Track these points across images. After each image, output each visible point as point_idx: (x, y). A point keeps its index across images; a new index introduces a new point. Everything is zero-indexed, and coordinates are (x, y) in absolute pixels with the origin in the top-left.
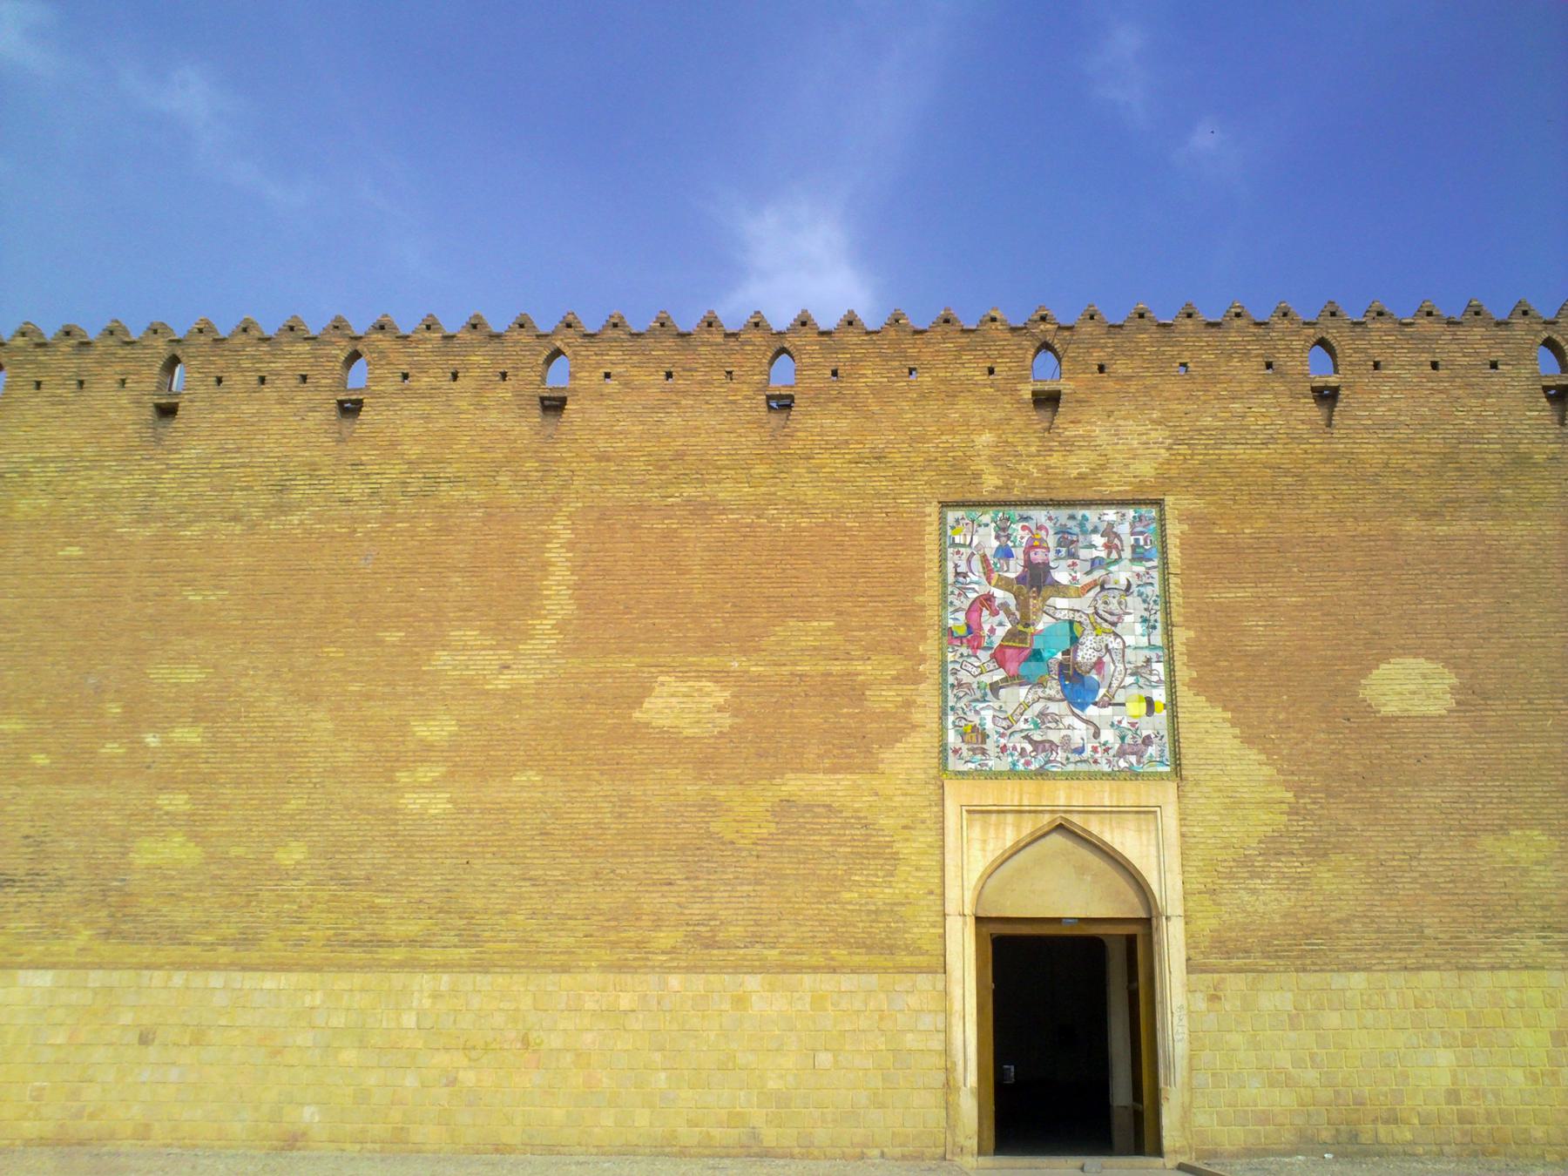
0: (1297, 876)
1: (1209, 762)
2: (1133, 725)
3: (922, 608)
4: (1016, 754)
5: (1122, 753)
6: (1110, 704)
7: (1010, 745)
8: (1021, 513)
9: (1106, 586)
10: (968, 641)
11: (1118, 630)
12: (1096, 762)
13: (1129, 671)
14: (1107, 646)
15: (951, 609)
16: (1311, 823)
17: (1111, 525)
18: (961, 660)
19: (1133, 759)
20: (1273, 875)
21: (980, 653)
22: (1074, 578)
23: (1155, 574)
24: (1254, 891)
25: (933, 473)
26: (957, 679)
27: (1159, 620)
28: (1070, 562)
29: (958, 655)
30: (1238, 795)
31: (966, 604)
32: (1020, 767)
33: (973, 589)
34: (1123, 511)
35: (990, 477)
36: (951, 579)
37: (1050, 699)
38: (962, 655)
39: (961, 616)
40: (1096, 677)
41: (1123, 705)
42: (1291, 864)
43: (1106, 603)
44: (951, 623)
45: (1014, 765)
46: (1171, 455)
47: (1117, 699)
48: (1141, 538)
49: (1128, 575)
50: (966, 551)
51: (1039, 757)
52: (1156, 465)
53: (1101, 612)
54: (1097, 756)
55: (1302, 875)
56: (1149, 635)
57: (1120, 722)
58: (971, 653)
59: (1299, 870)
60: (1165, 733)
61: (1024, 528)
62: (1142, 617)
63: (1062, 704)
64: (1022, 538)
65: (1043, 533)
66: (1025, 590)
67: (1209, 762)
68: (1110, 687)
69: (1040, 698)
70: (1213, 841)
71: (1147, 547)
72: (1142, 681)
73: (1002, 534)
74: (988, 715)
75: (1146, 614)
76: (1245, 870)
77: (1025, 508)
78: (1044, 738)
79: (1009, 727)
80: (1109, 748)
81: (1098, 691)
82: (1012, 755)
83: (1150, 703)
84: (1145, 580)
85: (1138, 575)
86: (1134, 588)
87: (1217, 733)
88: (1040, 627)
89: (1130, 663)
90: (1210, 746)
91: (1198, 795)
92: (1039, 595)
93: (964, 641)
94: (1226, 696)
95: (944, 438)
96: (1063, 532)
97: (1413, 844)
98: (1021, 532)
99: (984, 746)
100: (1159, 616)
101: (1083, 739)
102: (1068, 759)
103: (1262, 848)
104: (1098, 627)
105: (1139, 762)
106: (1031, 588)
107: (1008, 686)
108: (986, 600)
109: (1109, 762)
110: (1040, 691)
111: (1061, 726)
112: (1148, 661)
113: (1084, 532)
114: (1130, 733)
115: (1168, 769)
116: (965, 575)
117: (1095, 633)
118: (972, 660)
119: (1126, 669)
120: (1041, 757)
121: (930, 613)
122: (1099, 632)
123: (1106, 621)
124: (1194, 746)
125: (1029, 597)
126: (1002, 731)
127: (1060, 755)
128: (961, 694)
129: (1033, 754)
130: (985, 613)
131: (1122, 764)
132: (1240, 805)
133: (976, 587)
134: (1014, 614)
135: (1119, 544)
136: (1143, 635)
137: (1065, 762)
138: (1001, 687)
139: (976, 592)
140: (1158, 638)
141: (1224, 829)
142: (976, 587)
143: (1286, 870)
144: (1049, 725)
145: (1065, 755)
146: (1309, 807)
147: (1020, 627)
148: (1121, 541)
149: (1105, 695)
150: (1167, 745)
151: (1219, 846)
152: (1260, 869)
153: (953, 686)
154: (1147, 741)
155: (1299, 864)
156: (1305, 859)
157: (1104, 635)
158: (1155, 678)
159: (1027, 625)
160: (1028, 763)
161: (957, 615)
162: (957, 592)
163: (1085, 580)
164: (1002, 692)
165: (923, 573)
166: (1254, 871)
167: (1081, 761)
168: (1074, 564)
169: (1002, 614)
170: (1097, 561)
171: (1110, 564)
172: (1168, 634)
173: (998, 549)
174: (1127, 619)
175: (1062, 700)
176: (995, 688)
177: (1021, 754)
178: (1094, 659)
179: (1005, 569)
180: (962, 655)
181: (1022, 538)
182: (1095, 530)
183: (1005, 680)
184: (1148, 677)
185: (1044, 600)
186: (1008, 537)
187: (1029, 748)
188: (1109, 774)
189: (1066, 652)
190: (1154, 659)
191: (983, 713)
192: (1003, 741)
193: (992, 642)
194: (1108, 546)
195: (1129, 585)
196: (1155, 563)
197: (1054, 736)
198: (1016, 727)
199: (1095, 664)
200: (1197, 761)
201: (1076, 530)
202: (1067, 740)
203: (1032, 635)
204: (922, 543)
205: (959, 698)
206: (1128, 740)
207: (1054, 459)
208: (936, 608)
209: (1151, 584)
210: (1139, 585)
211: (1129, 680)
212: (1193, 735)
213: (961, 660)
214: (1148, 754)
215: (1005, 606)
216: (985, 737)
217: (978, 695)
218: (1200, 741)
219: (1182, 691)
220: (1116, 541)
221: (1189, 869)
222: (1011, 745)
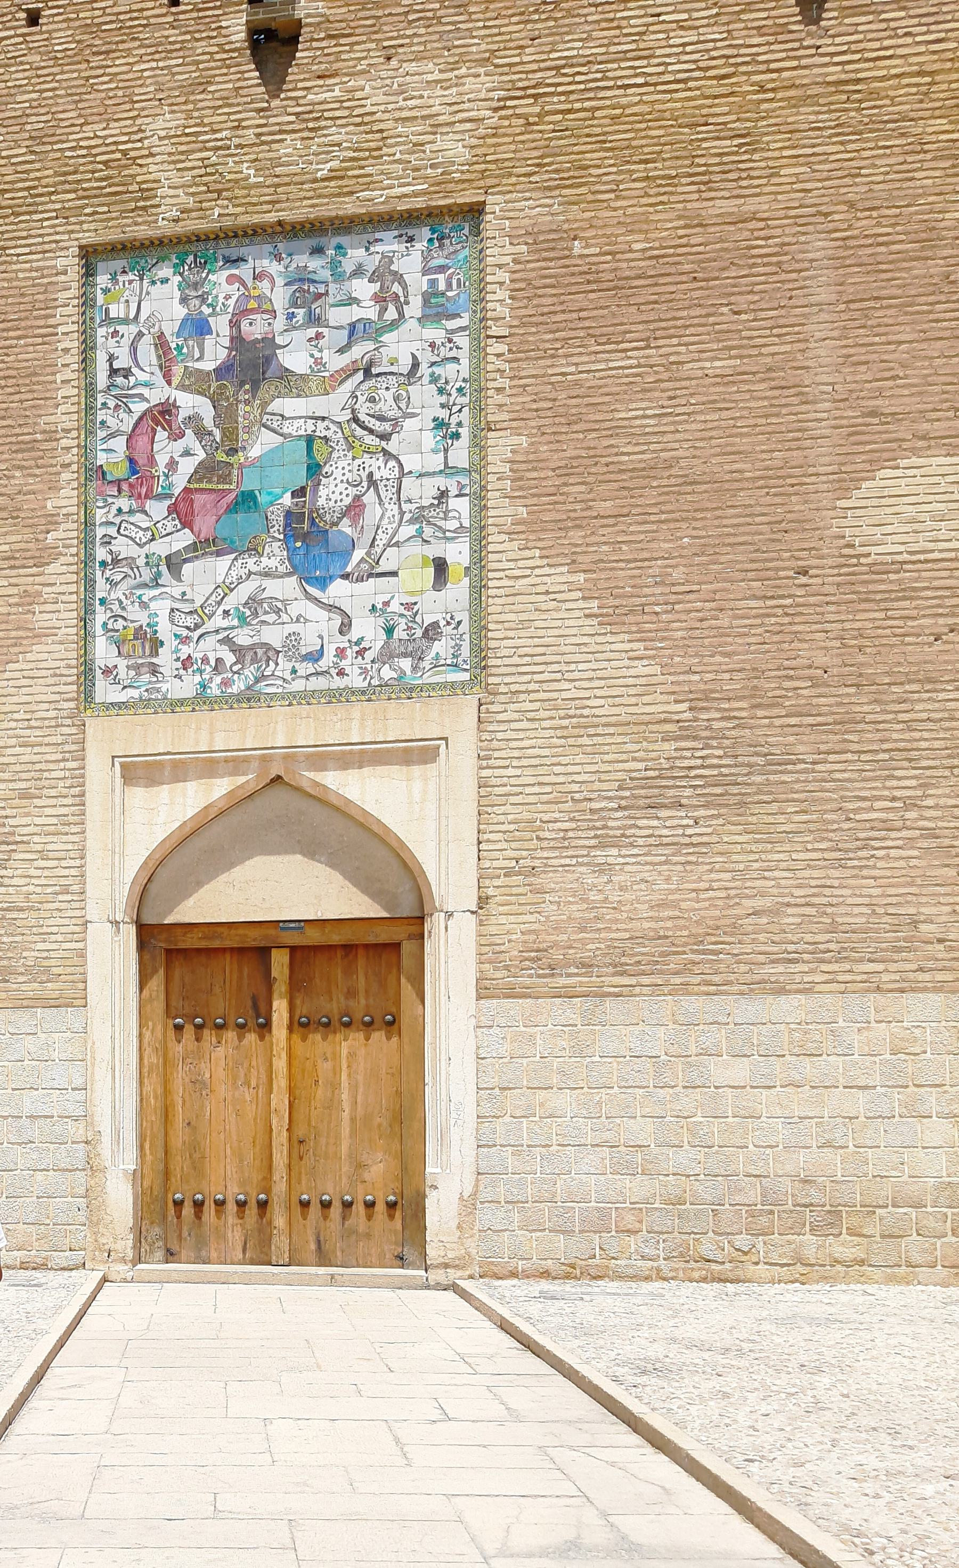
0: (687, 840)
1: (538, 659)
2: (409, 606)
3: (51, 435)
4: (208, 669)
5: (386, 656)
6: (370, 575)
7: (198, 655)
8: (227, 252)
9: (374, 371)
10: (131, 486)
11: (392, 446)
12: (341, 673)
13: (407, 516)
14: (371, 475)
15: (101, 434)
16: (720, 752)
17: (388, 259)
18: (117, 520)
19: (406, 664)
20: (641, 841)
21: (149, 505)
22: (318, 362)
23: (463, 340)
24: (603, 869)
25: (73, 196)
26: (111, 552)
27: (466, 422)
28: (311, 332)
29: (114, 510)
30: (586, 712)
31: (128, 423)
32: (214, 690)
33: (141, 397)
34: (411, 232)
35: (172, 192)
36: (102, 379)
37: (267, 574)
38: (120, 510)
39: (119, 444)
40: (348, 530)
41: (394, 574)
42: (675, 822)
43: (372, 400)
44: (102, 459)
45: (204, 687)
46: (500, 118)
47: (384, 566)
48: (441, 278)
49: (415, 347)
50: (128, 331)
51: (246, 672)
52: (474, 141)
53: (362, 417)
54: (343, 663)
55: (695, 840)
56: (446, 451)
57: (387, 604)
58: (135, 506)
59: (689, 831)
60: (464, 616)
61: (231, 279)
62: (435, 420)
63: (287, 580)
64: (227, 297)
65: (265, 285)
66: (230, 391)
67: (538, 659)
68: (372, 545)
69: (250, 573)
70: (536, 789)
71: (449, 294)
72: (428, 531)
73: (194, 293)
74: (162, 608)
75: (443, 414)
76: (592, 833)
77: (234, 242)
78: (256, 640)
79: (197, 626)
80: (365, 649)
81: (348, 554)
82: (201, 671)
83: (441, 566)
84: (444, 352)
85: (432, 345)
86: (424, 369)
87: (557, 610)
88: (255, 452)
89: (410, 501)
90: (541, 633)
91: (516, 716)
92: (254, 397)
93: (125, 487)
94: (576, 545)
95: (88, 131)
96: (301, 279)
97: (914, 783)
98: (226, 288)
99: (154, 660)
100: (465, 416)
101: (321, 637)
102: (294, 671)
103: (622, 798)
104: (357, 443)
105: (415, 668)
106: (242, 384)
107: (197, 557)
108: (162, 413)
109: (365, 672)
110: (251, 562)
111: (285, 618)
112: (443, 495)
113: (339, 277)
114: (404, 621)
115: (466, 676)
116: (127, 373)
117: (350, 455)
118: (138, 518)
119: (402, 513)
120: (250, 672)
121: (64, 442)
122: (358, 451)
123: (371, 431)
124: (511, 634)
125: (238, 401)
126: (185, 633)
127: (284, 666)
128: (118, 577)
129: (235, 668)
130: (161, 435)
131: (387, 673)
132: (592, 731)
133: (145, 392)
134: (210, 433)
135: (401, 294)
136: (435, 451)
137: (288, 676)
138: (186, 561)
139: (147, 401)
140: (460, 455)
141: (557, 769)
142: (145, 392)
143: (665, 832)
144: (264, 618)
145: (289, 666)
146: (716, 725)
147: (221, 456)
148: (405, 287)
149: (362, 560)
150: (466, 637)
151: (545, 798)
152: (618, 833)
153: (104, 564)
154: (432, 632)
155: (691, 822)
156: (702, 812)
157: (366, 455)
158: (452, 525)
159: (233, 451)
160: (226, 683)
161: (112, 444)
162: (111, 404)
163: (337, 362)
164: (187, 569)
165: (54, 374)
166: (608, 836)
167: (317, 674)
168: (319, 336)
169: (189, 432)
170: (360, 327)
171: (381, 331)
172: (478, 445)
173: (185, 321)
174: (408, 424)
175: (289, 575)
176: (174, 564)
177: (216, 669)
178: (348, 501)
179: (197, 355)
180: (120, 510)
181: (227, 297)
182: (358, 272)
183: (194, 547)
184: (441, 523)
185: (264, 405)
186: (203, 299)
187: (229, 658)
188: (363, 693)
189: (300, 493)
190: (454, 491)
191: (153, 605)
192: (185, 651)
193: (171, 485)
194: (380, 299)
195: (416, 365)
196: (463, 321)
197: (273, 636)
198: (210, 625)
199: (349, 508)
200: (516, 660)
201: (326, 274)
202: (293, 640)
203: (241, 467)
204: (51, 321)
205: (113, 584)
206: (400, 633)
207: (288, 148)
208: (74, 434)
209: (456, 359)
210: (433, 364)
211: (408, 530)
212: (512, 617)
213: (117, 520)
214: (433, 654)
215: (194, 420)
216: (157, 645)
217: (147, 575)
218: (524, 625)
219: (496, 540)
220: (396, 288)
221: (492, 837)
222: (201, 655)
